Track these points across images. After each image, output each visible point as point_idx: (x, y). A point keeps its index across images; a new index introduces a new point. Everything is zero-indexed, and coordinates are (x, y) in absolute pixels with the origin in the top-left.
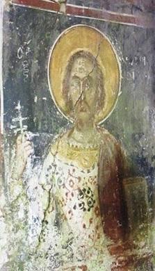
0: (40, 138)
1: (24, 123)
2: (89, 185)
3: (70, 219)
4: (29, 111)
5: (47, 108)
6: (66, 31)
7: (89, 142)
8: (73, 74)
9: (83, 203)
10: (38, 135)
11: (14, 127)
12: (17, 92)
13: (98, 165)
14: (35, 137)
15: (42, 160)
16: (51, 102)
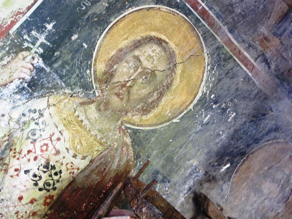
0: (48, 75)
1: (42, 45)
2: (63, 168)
3: (12, 176)
4: (58, 40)
5: (80, 56)
6: (164, 8)
7: (99, 131)
8: (137, 53)
9: (40, 178)
10: (48, 70)
11: (28, 39)
12: (59, 12)
13: (91, 161)
14: (43, 68)
15: (31, 97)
16: (89, 55)
